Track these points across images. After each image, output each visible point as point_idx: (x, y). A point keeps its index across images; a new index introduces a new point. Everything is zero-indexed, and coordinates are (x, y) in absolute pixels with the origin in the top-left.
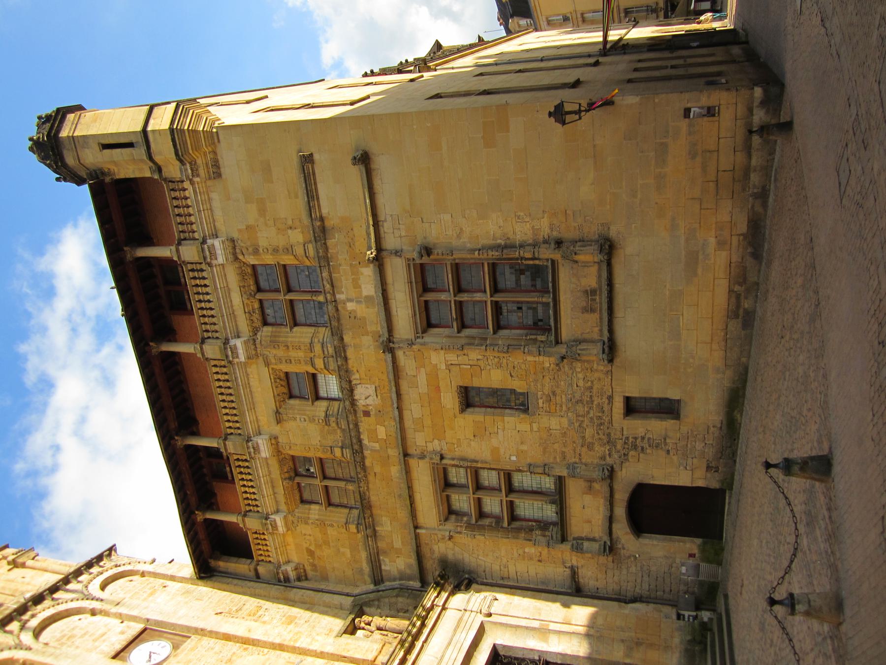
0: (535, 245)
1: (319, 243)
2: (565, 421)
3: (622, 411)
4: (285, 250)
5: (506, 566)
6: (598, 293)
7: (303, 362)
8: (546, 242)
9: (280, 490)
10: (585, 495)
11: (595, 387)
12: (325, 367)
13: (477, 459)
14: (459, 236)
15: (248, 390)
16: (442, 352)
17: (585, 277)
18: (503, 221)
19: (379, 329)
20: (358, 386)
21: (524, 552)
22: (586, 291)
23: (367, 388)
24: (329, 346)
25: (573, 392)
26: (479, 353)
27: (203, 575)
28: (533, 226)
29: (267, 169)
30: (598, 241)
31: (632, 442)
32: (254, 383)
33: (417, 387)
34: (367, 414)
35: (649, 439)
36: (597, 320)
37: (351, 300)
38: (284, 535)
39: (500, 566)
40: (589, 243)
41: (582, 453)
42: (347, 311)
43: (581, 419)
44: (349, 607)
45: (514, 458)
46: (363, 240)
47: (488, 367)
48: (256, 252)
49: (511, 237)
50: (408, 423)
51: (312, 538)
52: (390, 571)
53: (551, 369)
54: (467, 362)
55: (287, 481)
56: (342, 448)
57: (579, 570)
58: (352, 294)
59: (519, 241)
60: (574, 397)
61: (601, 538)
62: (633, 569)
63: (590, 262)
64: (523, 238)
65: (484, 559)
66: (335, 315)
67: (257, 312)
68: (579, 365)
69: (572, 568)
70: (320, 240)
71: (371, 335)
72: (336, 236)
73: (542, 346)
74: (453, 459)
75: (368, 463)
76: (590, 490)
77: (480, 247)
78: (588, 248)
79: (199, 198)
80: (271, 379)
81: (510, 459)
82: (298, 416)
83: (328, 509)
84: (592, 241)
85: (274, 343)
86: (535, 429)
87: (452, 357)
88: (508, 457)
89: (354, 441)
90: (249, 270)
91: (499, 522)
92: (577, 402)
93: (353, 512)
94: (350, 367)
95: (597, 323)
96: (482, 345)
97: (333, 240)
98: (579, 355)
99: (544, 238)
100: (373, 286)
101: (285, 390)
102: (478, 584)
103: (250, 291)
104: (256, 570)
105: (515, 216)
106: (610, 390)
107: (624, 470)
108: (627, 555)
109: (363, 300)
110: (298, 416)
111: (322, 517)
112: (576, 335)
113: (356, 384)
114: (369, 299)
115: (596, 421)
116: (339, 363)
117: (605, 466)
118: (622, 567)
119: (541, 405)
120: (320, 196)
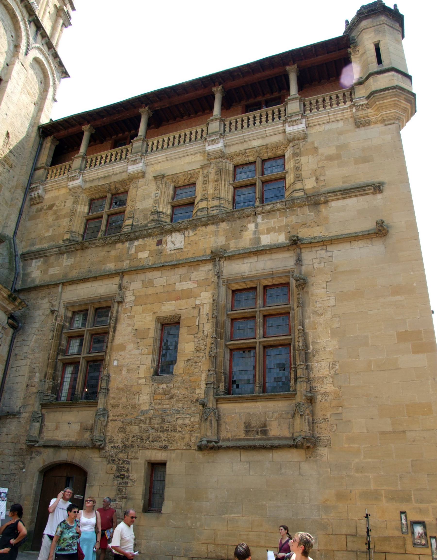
0: (309, 380)
1: (305, 200)
2: (145, 407)
3: (153, 459)
4: (298, 175)
5: (25, 358)
6: (264, 437)
7: (203, 193)
8: (312, 388)
9: (102, 183)
10: (80, 424)
11: (176, 435)
12: (200, 209)
13: (117, 332)
14: (315, 313)
15: (182, 155)
16: (211, 301)
17: (279, 425)
18: (330, 351)
19: (232, 250)
20: (183, 235)
21: (36, 373)
22: (266, 426)
23: (181, 242)
24: (218, 211)
25: (172, 415)
27: (41, 129)
29: (365, 160)
30: (313, 437)
31: (125, 468)
32: (188, 159)
33: (180, 282)
34: (159, 243)
35: (127, 483)
37: (257, 226)
38: (66, 187)
39: (26, 353)
40: (312, 428)
41: (117, 422)
42: (247, 224)
43: (147, 421)
44: (5, 232)
45: (115, 363)
46: (309, 234)
47: (196, 340)
48: (296, 155)
49: (315, 358)
50: (150, 275)
51: (62, 207)
52: (31, 266)
53: (194, 395)
54: (202, 322)
55: (108, 187)
56: (132, 225)
57: (16, 419)
58: (262, 227)
59: (312, 365)
60: (168, 415)
61: (43, 438)
62: (13, 467)
63: (293, 429)
64: (315, 368)
65: (33, 340)
66: (244, 215)
67: (246, 159)
68: (197, 420)
69: (19, 413)
70: (308, 201)
71: (227, 243)
73: (215, 387)
74: (117, 312)
75: (119, 245)
76: (84, 429)
77: (306, 330)
78: (307, 427)
79: (339, 112)
80: (191, 170)
81: (115, 360)
82: (159, 192)
83: (84, 219)
84: (313, 430)
85: (220, 171)
86: (140, 381)
87: (206, 309)
88: (117, 358)
89: (137, 234)
90: (279, 153)
91: (63, 352)
92: (163, 418)
93: (80, 237)
94: (200, 228)
95: (235, 436)
96: (216, 334)
97: (308, 211)
98: (206, 419)
99: (315, 387)
100: (269, 243)
101: (181, 183)
102: (13, 334)
103: (263, 154)
104: (41, 168)
105: (336, 361)
106: (172, 448)
107: (99, 460)
108: (25, 461)
109: (257, 236)
110: (159, 192)
111: (78, 214)
112: (225, 417)
113: (184, 234)
114: (258, 240)
115: (145, 434)
116: (203, 219)
117: (104, 442)
118: (15, 457)
119: (162, 386)
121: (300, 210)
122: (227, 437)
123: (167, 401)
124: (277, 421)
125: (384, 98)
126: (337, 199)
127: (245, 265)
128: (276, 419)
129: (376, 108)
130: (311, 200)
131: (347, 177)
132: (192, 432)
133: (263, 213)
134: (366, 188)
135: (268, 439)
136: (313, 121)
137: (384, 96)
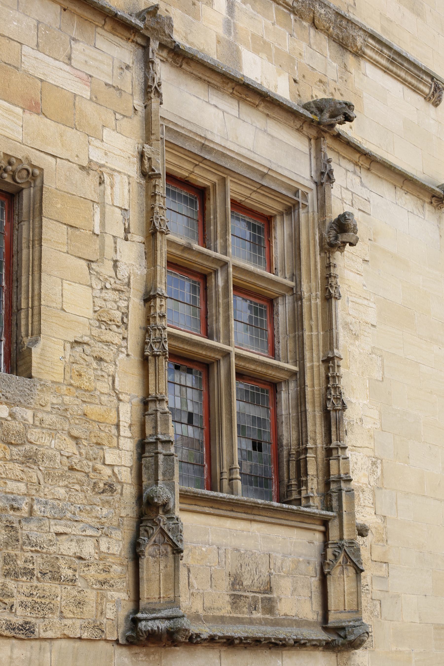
6: (268, 616)
17: (295, 590)
22: (270, 590)
26: (135, 275)
28: (363, 491)
36: (218, 609)
47: (98, 285)
53: (99, 466)
72: (335, 65)
95: (210, 608)
97: (328, 54)
105: (377, 458)
106: (50, 634)
120: (386, 77)
121: (315, 36)
122: (193, 610)
123: (17, 467)
124: (290, 580)
126: (376, 64)
127: (214, 110)
128: (288, 575)
132: (105, 587)
135: (276, 623)
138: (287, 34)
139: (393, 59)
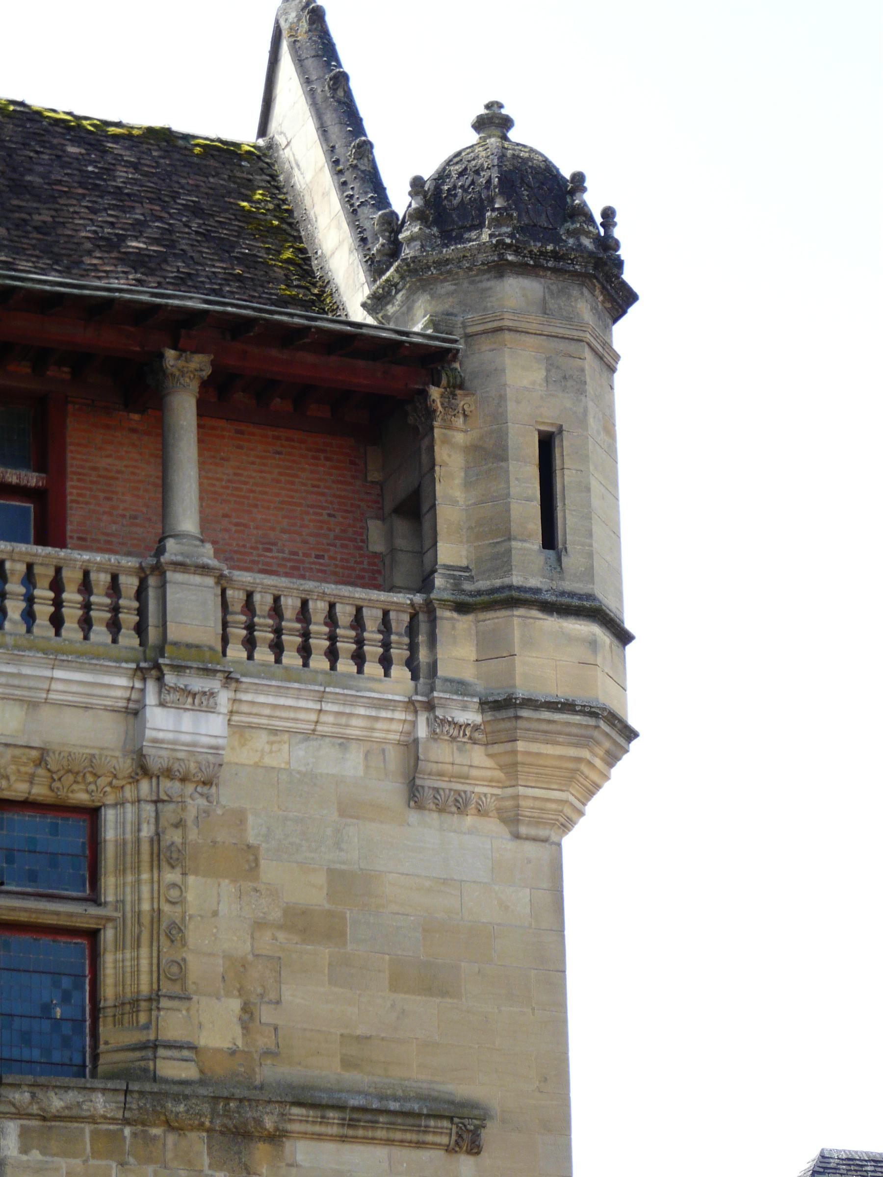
1: (206, 1108)
70: (214, 1113)
79: (362, 711)
120: (347, 1147)
125: (548, 737)
126: (319, 1137)
129: (507, 760)
130: (227, 1114)
131: (359, 1038)
133: (30, 1116)
134: (432, 1123)
136: (255, 710)
137: (551, 727)
138: (114, 1165)
139: (351, 1120)
